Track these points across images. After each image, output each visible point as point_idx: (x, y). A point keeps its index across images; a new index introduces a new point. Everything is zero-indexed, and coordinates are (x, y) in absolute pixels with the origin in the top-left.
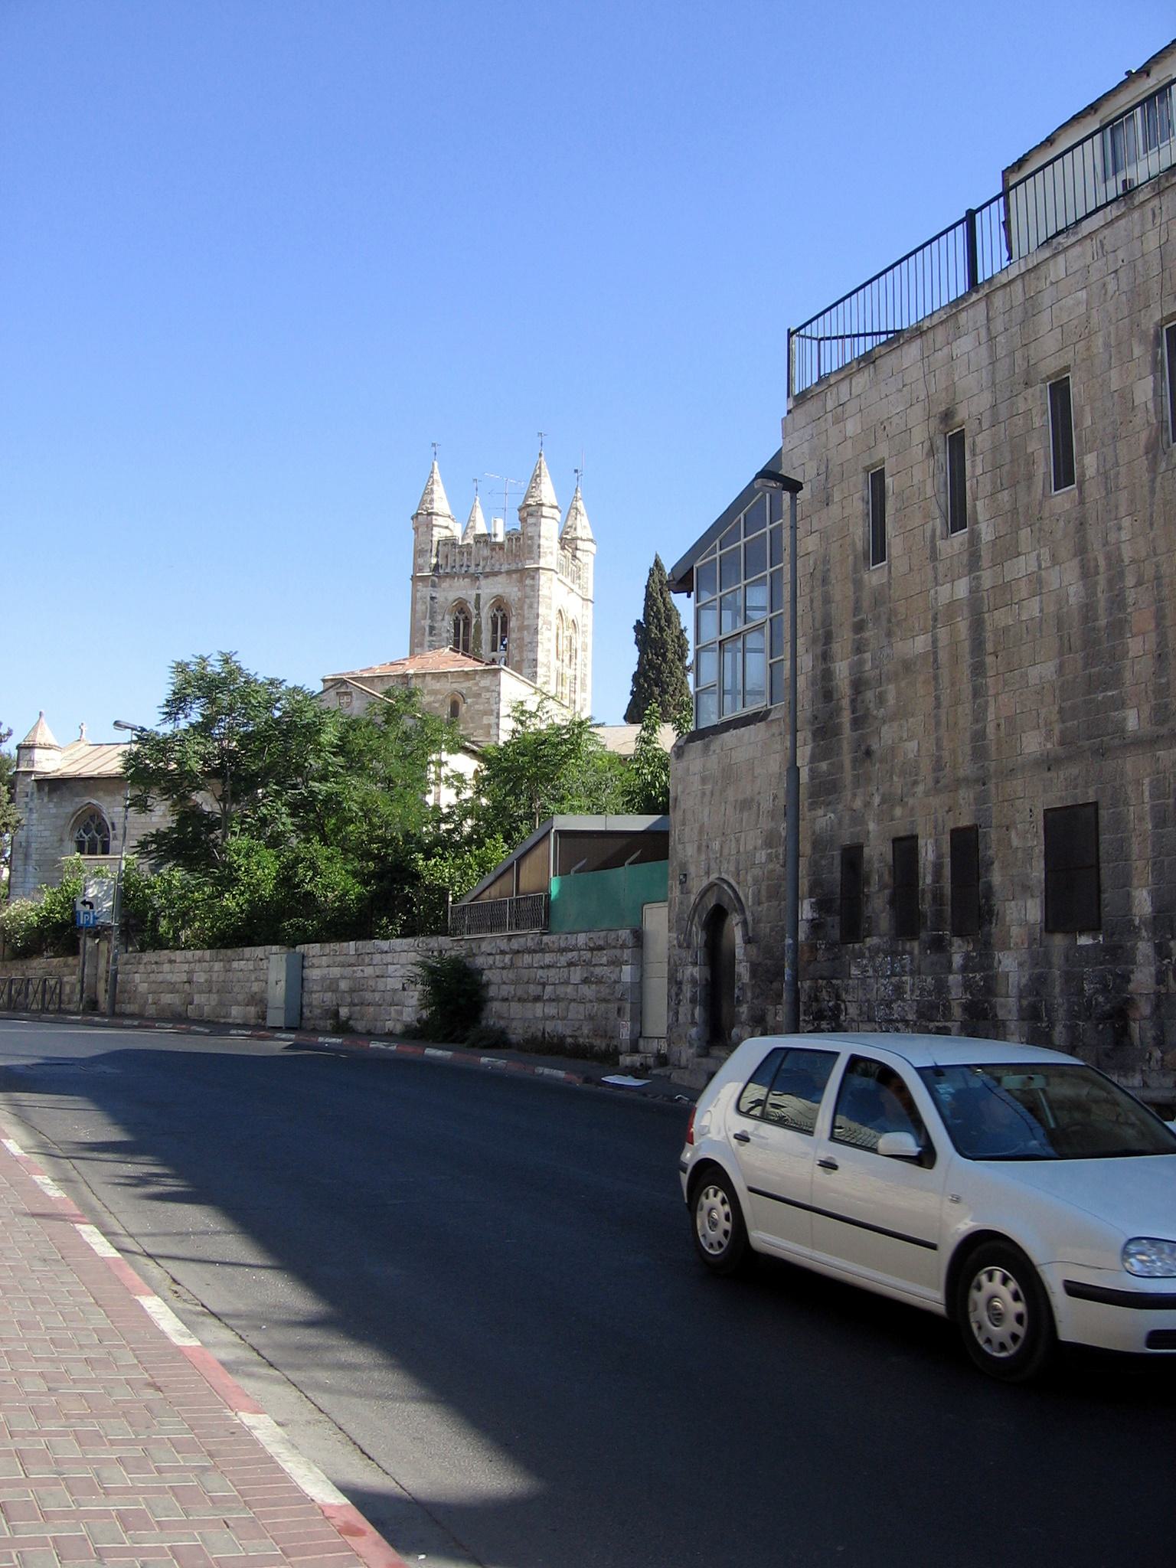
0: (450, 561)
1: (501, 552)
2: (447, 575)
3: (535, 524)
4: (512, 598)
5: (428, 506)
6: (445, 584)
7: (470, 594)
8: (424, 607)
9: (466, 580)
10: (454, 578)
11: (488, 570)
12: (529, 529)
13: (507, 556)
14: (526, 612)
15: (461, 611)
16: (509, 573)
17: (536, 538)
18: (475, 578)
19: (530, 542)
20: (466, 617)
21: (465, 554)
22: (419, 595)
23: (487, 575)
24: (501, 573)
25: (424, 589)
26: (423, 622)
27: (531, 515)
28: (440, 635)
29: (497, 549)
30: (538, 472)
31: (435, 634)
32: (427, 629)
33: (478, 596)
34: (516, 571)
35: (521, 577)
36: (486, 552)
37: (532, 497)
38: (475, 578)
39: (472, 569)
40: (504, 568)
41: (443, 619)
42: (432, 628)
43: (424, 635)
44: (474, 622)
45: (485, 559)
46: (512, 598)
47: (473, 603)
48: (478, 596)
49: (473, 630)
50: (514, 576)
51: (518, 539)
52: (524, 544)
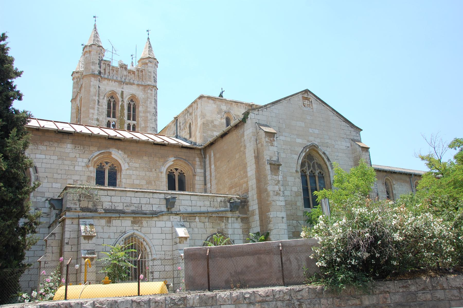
0: (107, 71)
1: (133, 75)
2: (105, 79)
6: (105, 82)
7: (118, 90)
8: (95, 90)
9: (116, 83)
10: (110, 80)
11: (127, 81)
12: (149, 68)
14: (149, 105)
15: (112, 97)
16: (138, 85)
19: (149, 74)
20: (115, 101)
21: (115, 71)
22: (92, 83)
23: (127, 84)
24: (134, 84)
25: (95, 81)
26: (94, 97)
27: (151, 62)
28: (102, 106)
29: (132, 74)
32: (97, 101)
33: (122, 92)
34: (142, 85)
35: (145, 88)
36: (125, 73)
39: (119, 79)
41: (104, 99)
43: (95, 104)
44: (120, 103)
45: (126, 76)
47: (120, 94)
48: (122, 92)
49: (120, 108)
50: (140, 87)
51: (142, 71)
52: (146, 74)
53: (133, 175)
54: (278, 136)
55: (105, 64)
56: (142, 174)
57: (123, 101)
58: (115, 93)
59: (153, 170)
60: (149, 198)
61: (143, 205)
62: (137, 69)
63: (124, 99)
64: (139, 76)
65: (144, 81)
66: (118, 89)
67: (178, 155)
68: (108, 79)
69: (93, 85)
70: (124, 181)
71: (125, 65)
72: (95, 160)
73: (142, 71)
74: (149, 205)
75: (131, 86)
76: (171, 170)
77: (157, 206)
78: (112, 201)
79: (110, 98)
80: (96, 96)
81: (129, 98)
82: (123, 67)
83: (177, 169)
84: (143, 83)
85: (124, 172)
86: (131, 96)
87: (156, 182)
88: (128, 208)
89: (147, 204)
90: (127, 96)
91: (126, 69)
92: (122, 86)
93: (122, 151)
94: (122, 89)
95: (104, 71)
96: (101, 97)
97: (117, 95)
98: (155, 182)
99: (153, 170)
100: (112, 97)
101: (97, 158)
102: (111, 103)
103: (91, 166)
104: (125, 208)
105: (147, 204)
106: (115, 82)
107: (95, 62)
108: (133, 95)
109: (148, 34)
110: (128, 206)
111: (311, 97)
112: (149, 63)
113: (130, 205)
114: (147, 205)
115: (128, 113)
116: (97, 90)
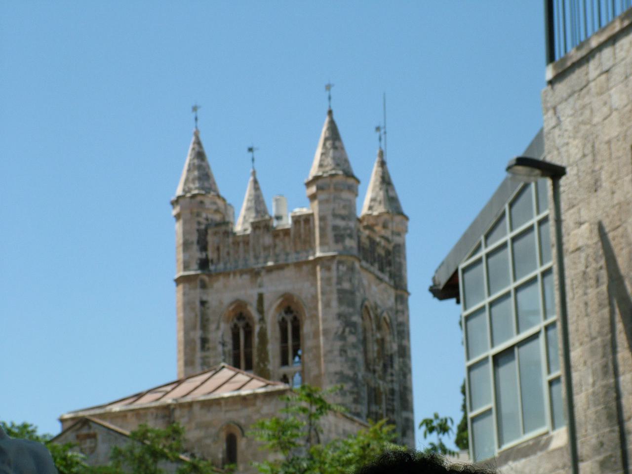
0: (223, 253)
1: (287, 239)
6: (219, 284)
13: (295, 244)
18: (255, 274)
21: (241, 245)
23: (270, 270)
24: (287, 265)
28: (215, 348)
31: (208, 349)
33: (261, 298)
36: (267, 240)
38: (255, 274)
40: (292, 258)
41: (218, 328)
42: (204, 341)
44: (257, 329)
48: (261, 298)
57: (262, 320)
62: (295, 219)
63: (265, 314)
64: (300, 236)
68: (226, 274)
90: (271, 305)
92: (259, 280)
96: (212, 327)
111: (97, 431)
112: (320, 192)
116: (199, 313)
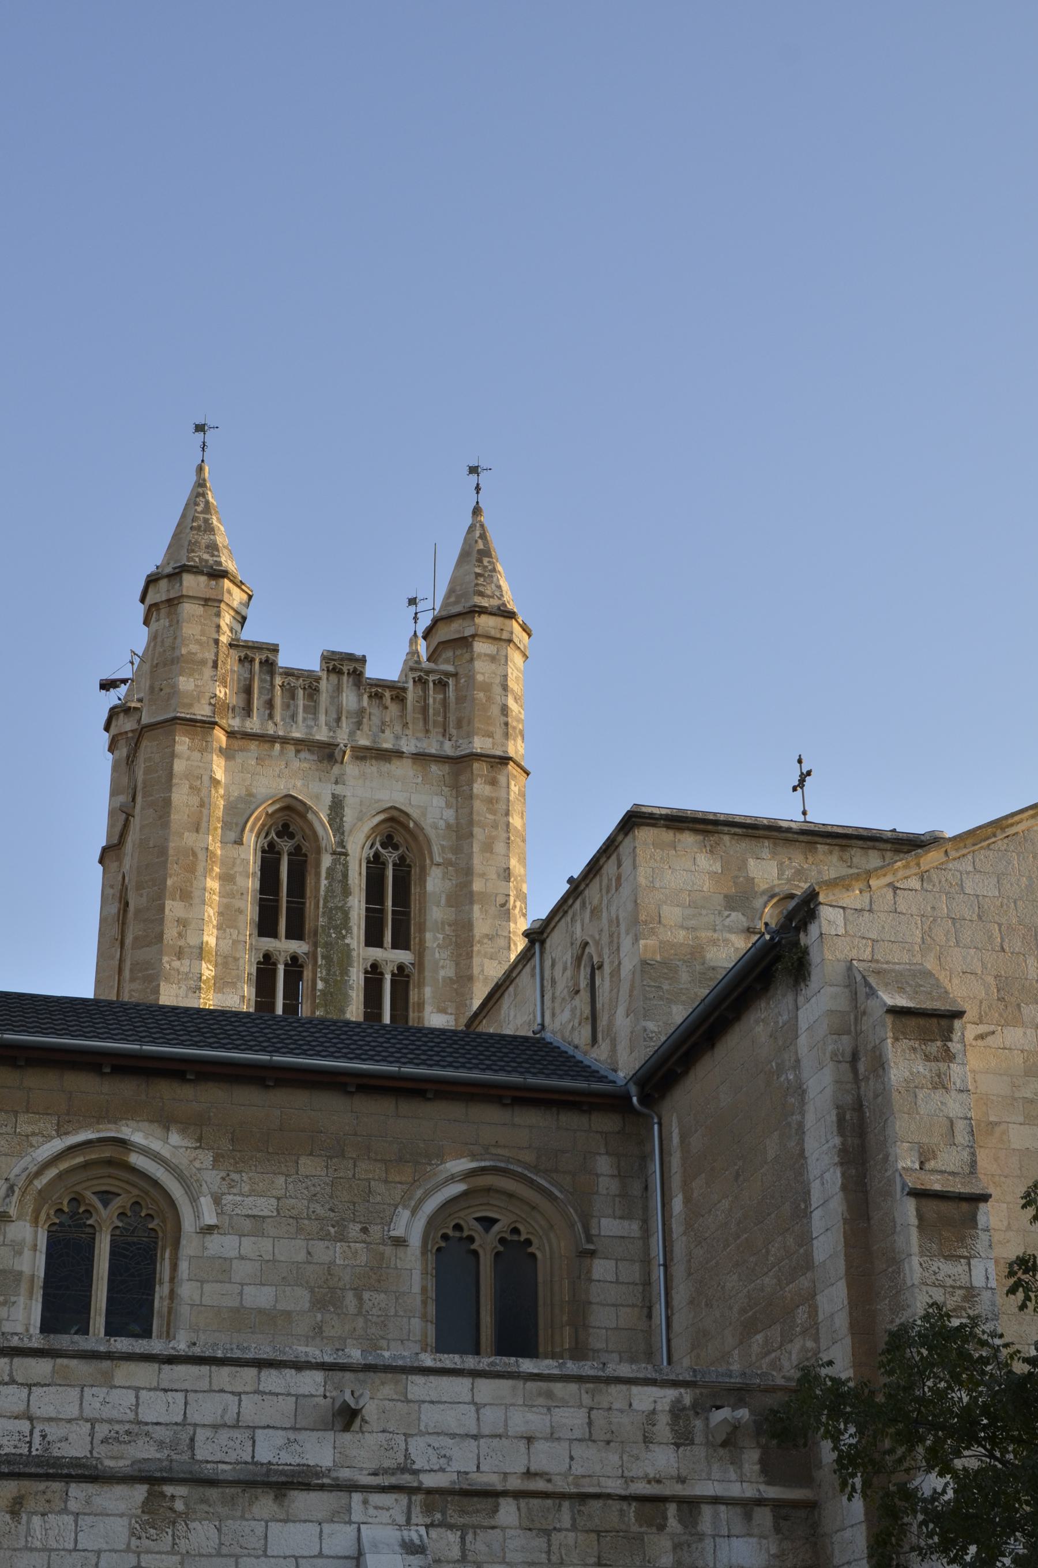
1: (394, 708)
3: (493, 659)
4: (430, 821)
5: (206, 556)
16: (421, 758)
17: (497, 690)
20: (298, 848)
24: (399, 754)
30: (480, 545)
37: (481, 594)
44: (327, 861)
46: (430, 821)
50: (434, 768)
53: (242, 1258)
54: (992, 1028)
55: (247, 664)
56: (292, 1250)
58: (300, 808)
59: (354, 1230)
60: (239, 1394)
61: (201, 1435)
62: (417, 674)
64: (425, 710)
65: (454, 732)
66: (315, 787)
67: (497, 1145)
69: (187, 776)
70: (187, 1291)
71: (351, 658)
72: (39, 1183)
73: (440, 681)
74: (236, 1434)
75: (385, 767)
76: (458, 1227)
77: (279, 1438)
78: (35, 1411)
79: (273, 834)
80: (197, 831)
81: (374, 829)
82: (340, 673)
83: (488, 1222)
84: (448, 749)
85: (189, 1246)
86: (381, 817)
87: (366, 1295)
88: (116, 1448)
89: (225, 1425)
91: (357, 675)
92: (336, 770)
93: (183, 1131)
94: (336, 783)
95: (243, 696)
97: (310, 816)
98: (360, 1299)
99: (354, 1230)
100: (285, 831)
101: (52, 1173)
102: (278, 861)
103: (19, 1218)
104: (101, 1451)
105: (225, 1425)
106: (298, 751)
107: (200, 656)
108: (395, 813)
109: (478, 489)
110: (117, 1439)
113: (128, 1433)
114: (224, 1435)
115: (367, 909)
